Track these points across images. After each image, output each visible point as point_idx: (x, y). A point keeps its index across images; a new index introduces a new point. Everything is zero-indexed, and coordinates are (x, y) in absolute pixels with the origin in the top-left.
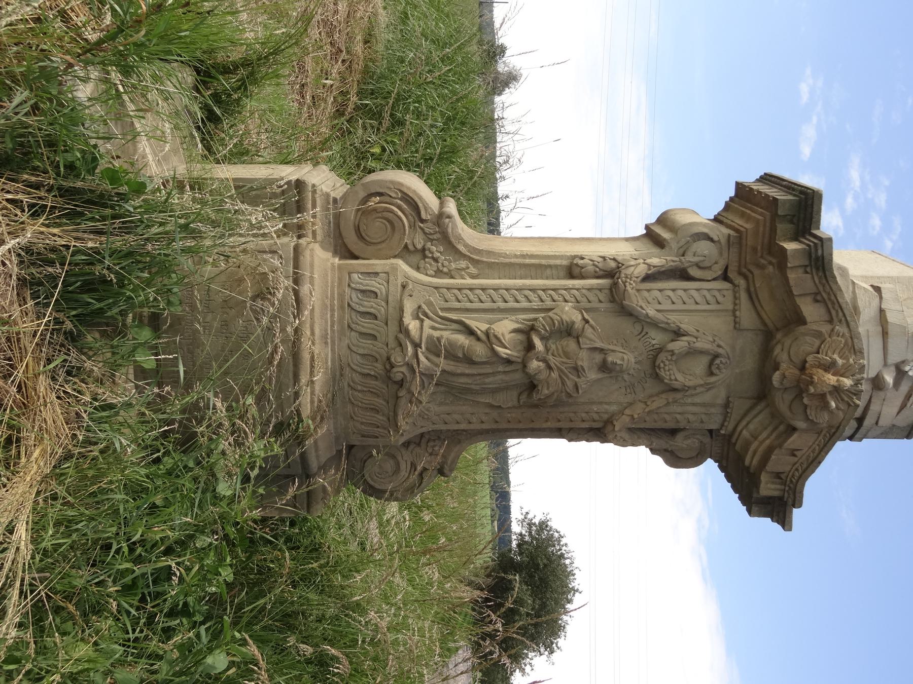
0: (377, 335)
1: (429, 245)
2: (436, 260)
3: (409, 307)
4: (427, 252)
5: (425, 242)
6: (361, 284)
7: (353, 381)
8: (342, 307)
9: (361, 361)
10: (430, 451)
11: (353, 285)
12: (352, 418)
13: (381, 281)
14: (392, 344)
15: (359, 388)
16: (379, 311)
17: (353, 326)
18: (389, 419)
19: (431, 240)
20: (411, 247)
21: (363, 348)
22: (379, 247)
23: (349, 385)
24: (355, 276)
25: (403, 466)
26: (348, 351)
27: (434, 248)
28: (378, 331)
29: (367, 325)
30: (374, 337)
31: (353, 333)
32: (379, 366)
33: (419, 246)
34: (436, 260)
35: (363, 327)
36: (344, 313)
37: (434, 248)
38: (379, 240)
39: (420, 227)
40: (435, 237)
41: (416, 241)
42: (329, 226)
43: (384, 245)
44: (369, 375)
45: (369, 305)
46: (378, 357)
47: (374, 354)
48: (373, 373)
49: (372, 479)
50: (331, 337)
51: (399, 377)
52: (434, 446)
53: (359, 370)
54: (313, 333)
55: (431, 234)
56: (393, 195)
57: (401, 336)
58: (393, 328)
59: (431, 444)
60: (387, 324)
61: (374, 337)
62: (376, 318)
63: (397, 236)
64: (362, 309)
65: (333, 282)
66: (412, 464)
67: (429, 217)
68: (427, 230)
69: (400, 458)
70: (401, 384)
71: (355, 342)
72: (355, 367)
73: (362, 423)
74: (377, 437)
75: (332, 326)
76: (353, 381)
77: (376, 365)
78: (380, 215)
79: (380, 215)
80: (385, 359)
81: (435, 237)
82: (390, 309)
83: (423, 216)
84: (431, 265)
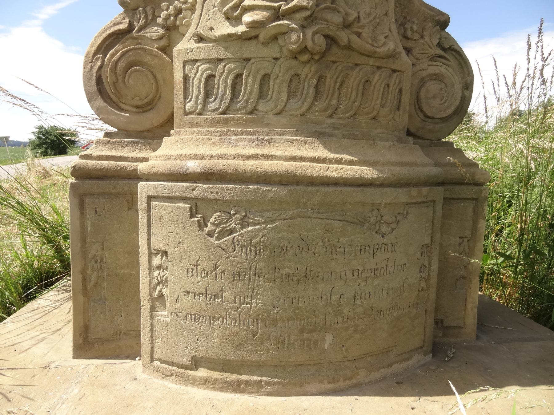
0: (262, 73)
1: (160, 20)
2: (179, 12)
3: (226, 29)
4: (169, 22)
5: (157, 25)
6: (197, 97)
7: (325, 110)
8: (226, 122)
9: (299, 97)
10: (417, 36)
11: (199, 107)
12: (374, 118)
13: (194, 71)
14: (273, 51)
15: (334, 102)
16: (230, 71)
17: (250, 107)
18: (379, 68)
19: (155, 17)
20: (163, 42)
21: (279, 92)
22: (161, 82)
23: (331, 116)
24: (189, 106)
25: (434, 70)
26: (284, 113)
27: (164, 14)
28: (258, 72)
29: (249, 86)
30: (265, 78)
31: (260, 107)
32: (305, 71)
33: (161, 31)
34: (179, 12)
35: (251, 92)
36: (233, 119)
37: (164, 14)
38: (152, 80)
39: (139, 30)
40: (150, 12)
41: (155, 36)
42: (138, 143)
43: (159, 76)
44: (317, 87)
45: (223, 85)
46: (292, 72)
47: (287, 78)
48: (315, 81)
49: (448, 108)
50: (264, 135)
51: (321, 41)
52: (412, 29)
53: (309, 100)
54: (254, 157)
55: (146, 17)
56: (99, 63)
57: (263, 35)
58: (252, 50)
59: (409, 33)
60: (248, 60)
61: (265, 78)
62: (239, 76)
63: (148, 59)
64: (228, 95)
65: (193, 133)
66: (430, 60)
67: (127, 20)
68: (142, 22)
69: (424, 74)
70: (331, 40)
71: (271, 105)
72: (306, 106)
73: (383, 106)
74: (401, 90)
75: (249, 133)
76: (325, 110)
77: (303, 76)
78: (120, 78)
79: (120, 78)
80: (295, 62)
81: (150, 12)
82: (228, 55)
83: (123, 26)
84: (184, 18)
